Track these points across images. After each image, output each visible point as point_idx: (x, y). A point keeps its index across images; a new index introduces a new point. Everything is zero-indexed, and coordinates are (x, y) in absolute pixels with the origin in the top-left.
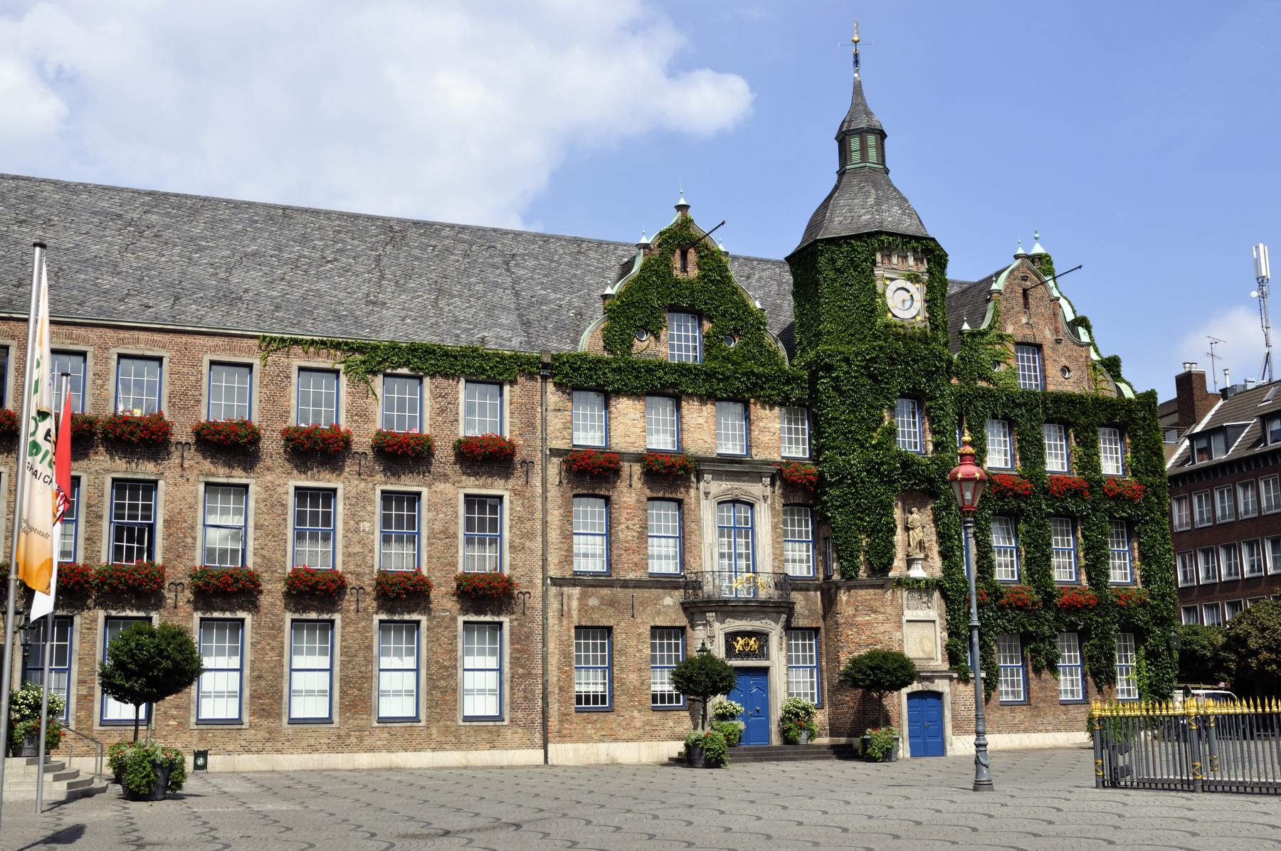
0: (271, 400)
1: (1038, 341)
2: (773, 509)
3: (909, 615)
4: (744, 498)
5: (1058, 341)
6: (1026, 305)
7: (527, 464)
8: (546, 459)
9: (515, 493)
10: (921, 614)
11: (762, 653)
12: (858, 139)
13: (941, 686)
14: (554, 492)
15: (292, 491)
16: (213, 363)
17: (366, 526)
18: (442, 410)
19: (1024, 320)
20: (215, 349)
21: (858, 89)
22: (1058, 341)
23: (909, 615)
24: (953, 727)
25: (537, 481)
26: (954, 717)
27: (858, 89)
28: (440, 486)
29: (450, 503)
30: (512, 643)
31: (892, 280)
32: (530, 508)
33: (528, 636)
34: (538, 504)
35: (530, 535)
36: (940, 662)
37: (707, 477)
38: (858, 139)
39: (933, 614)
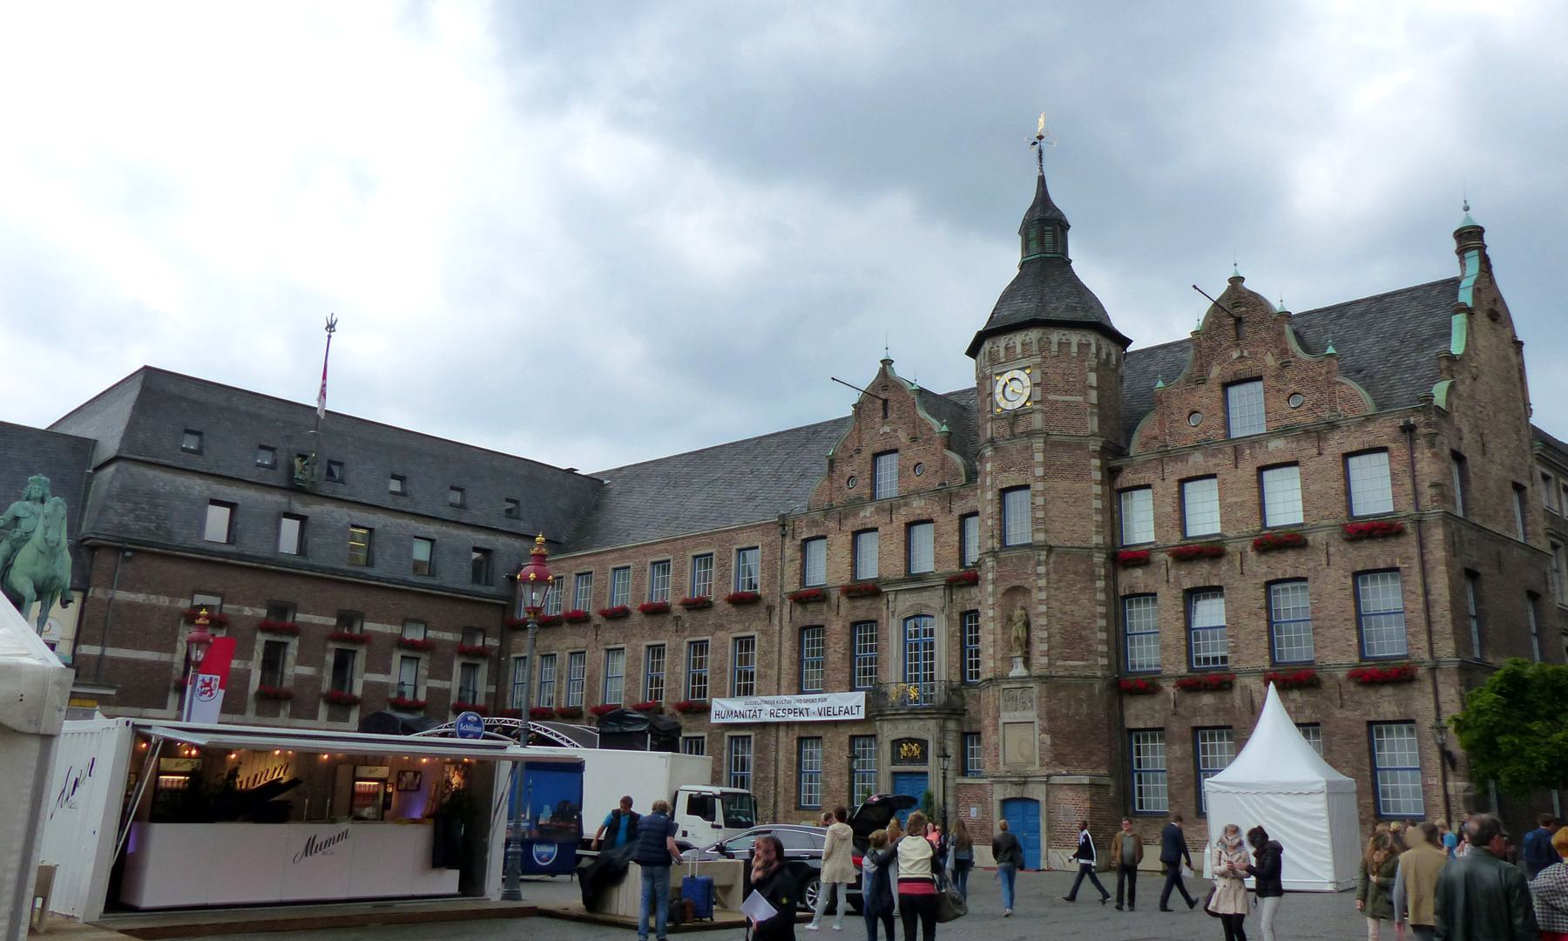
0: (638, 588)
1: (1254, 374)
2: (949, 617)
3: (1006, 717)
4: (925, 612)
5: (1284, 365)
6: (1238, 336)
7: (770, 609)
8: (782, 603)
9: (764, 632)
10: (1019, 716)
11: (924, 758)
12: (1045, 230)
13: (1037, 792)
14: (787, 629)
15: (644, 648)
16: (615, 569)
17: (678, 669)
18: (722, 576)
19: (1235, 355)
20: (615, 560)
21: (1042, 181)
22: (1284, 365)
23: (1006, 717)
24: (1050, 839)
25: (776, 621)
26: (1049, 828)
27: (1042, 181)
28: (720, 634)
29: (724, 645)
30: (757, 751)
31: (1001, 374)
32: (770, 642)
33: (767, 747)
34: (776, 639)
35: (769, 666)
36: (1037, 767)
37: (891, 597)
38: (1045, 230)
39: (1031, 715)
